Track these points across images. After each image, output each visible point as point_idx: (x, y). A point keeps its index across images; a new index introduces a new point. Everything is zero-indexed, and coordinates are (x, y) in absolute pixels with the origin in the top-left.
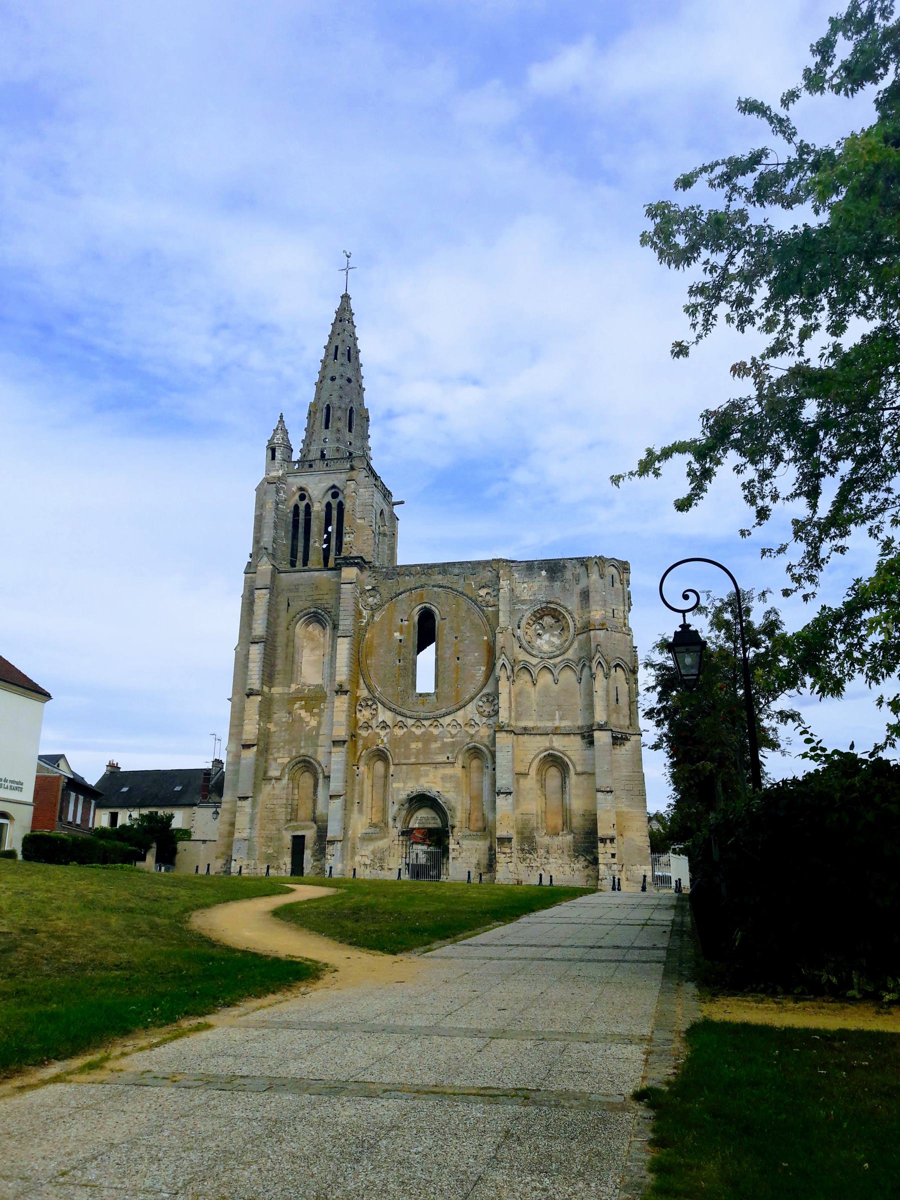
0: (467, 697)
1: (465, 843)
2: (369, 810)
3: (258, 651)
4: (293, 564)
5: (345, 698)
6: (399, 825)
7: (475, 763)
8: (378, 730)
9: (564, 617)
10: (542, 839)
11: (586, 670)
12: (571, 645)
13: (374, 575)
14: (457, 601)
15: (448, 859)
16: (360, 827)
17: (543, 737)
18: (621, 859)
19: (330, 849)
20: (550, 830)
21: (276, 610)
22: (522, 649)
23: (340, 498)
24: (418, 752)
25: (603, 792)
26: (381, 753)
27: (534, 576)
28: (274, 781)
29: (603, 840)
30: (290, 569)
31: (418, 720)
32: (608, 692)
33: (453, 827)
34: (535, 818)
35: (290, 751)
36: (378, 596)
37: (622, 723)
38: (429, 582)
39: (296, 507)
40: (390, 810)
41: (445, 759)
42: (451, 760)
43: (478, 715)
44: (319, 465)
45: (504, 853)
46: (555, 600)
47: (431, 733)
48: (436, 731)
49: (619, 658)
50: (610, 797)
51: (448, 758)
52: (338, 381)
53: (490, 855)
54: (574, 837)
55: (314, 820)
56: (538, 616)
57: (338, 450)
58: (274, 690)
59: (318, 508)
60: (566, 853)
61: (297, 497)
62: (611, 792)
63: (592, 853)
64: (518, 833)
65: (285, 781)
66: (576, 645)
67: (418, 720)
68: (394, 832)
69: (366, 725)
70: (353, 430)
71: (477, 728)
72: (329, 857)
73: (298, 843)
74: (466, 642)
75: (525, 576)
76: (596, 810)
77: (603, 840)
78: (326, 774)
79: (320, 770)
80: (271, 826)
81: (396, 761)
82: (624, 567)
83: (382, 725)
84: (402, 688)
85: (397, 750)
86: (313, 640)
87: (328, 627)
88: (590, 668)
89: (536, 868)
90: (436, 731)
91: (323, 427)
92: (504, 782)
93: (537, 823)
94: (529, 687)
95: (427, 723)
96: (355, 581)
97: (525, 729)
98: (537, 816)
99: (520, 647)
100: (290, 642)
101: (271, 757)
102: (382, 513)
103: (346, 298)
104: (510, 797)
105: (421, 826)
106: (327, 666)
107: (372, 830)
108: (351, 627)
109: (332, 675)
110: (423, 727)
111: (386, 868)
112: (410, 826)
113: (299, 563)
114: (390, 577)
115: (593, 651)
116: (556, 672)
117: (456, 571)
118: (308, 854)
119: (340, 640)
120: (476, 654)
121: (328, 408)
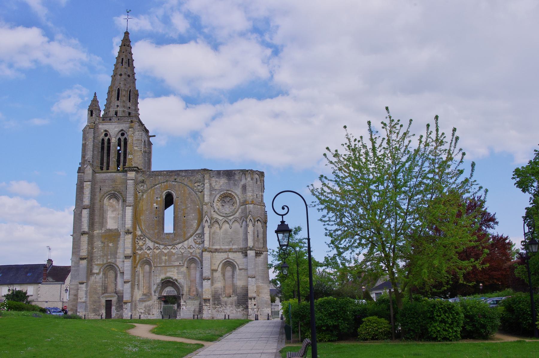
1: (189, 302)
2: (142, 287)
3: (87, 213)
4: (102, 168)
5: (130, 236)
6: (157, 294)
7: (193, 265)
8: (146, 251)
9: (235, 197)
10: (224, 299)
11: (244, 222)
12: (238, 211)
13: (143, 175)
15: (180, 309)
17: (224, 253)
18: (258, 307)
19: (125, 306)
20: (226, 294)
21: (94, 191)
23: (125, 136)
24: (166, 261)
25: (251, 277)
26: (148, 261)
28: (95, 275)
29: (251, 299)
30: (100, 171)
32: (254, 233)
33: (182, 295)
35: (103, 261)
37: (260, 246)
39: (103, 140)
40: (153, 288)
41: (179, 264)
44: (115, 119)
45: (206, 306)
46: (231, 189)
47: (172, 252)
48: (174, 251)
49: (259, 217)
50: (254, 279)
52: (123, 76)
53: (200, 307)
54: (238, 297)
55: (116, 293)
56: (223, 196)
57: (124, 111)
58: (95, 232)
59: (114, 140)
60: (234, 305)
61: (103, 135)
62: (255, 277)
63: (246, 304)
64: (212, 297)
65: (101, 275)
66: (240, 211)
68: (155, 297)
69: (140, 248)
70: (131, 101)
71: (194, 250)
72: (125, 310)
73: (109, 304)
74: (188, 209)
75: (217, 178)
76: (248, 285)
77: (251, 299)
78: (121, 271)
79: (118, 270)
80: (95, 296)
82: (262, 174)
86: (112, 207)
87: (120, 201)
88: (246, 222)
89: (220, 312)
91: (116, 99)
93: (221, 292)
95: (170, 247)
96: (134, 179)
97: (216, 249)
98: (221, 289)
99: (214, 212)
100: (102, 207)
101: (94, 263)
102: (145, 141)
104: (210, 281)
105: (167, 294)
106: (120, 220)
107: (144, 297)
109: (124, 224)
111: (151, 314)
112: (162, 295)
113: (105, 168)
115: (248, 214)
116: (231, 224)
118: (113, 308)
119: (127, 208)
120: (193, 215)
121: (119, 90)
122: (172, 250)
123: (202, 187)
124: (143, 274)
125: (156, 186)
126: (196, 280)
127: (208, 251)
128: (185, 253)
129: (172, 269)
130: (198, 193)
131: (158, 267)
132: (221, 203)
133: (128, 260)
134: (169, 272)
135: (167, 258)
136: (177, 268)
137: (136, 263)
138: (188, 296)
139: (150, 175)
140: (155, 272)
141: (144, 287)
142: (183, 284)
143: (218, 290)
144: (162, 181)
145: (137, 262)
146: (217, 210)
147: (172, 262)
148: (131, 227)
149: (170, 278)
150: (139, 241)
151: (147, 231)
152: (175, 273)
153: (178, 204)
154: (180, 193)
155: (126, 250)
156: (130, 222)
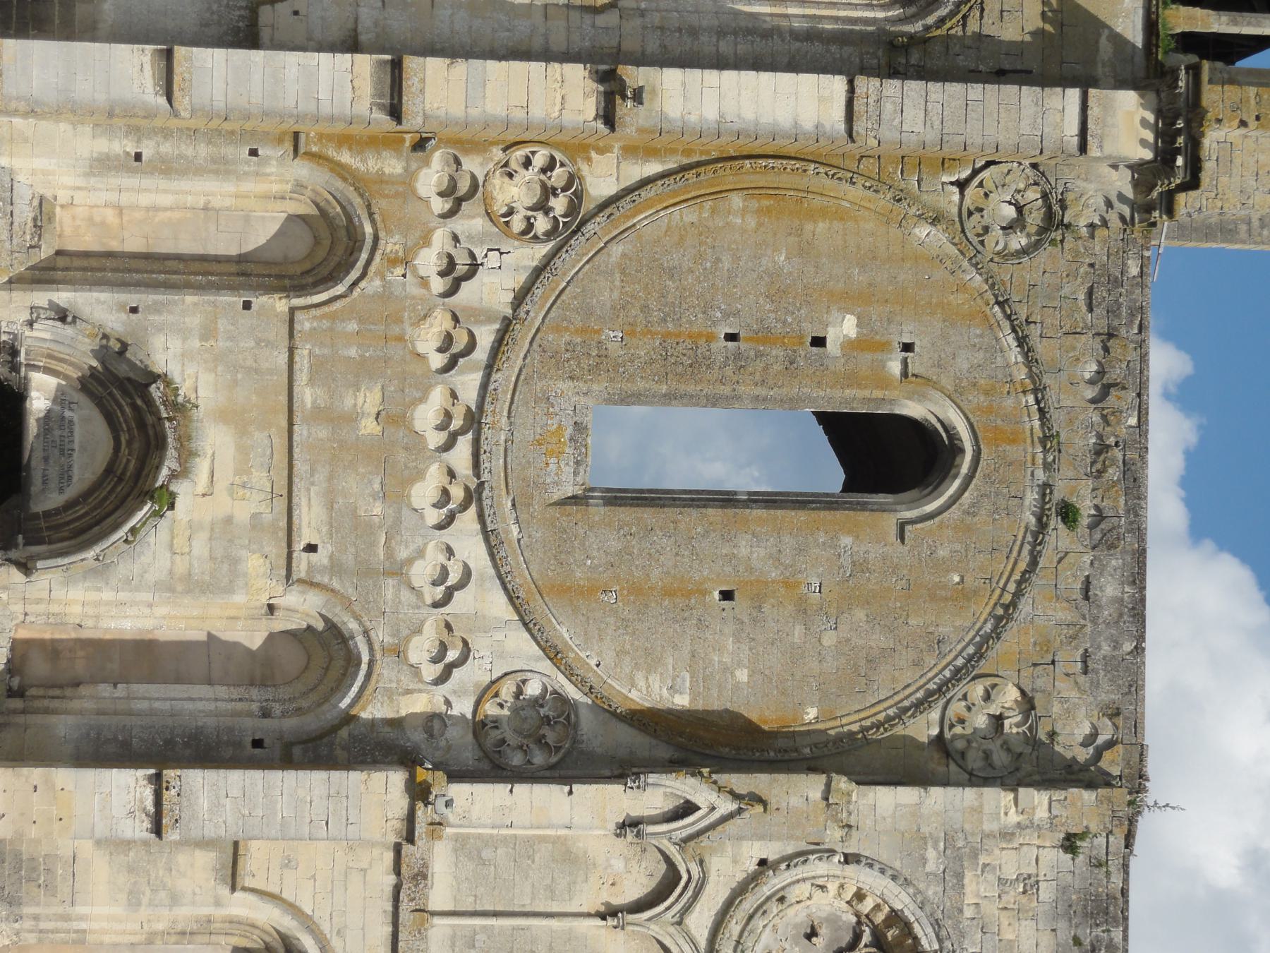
0: (564, 632)
2: (113, 197)
8: (440, 239)
14: (976, 592)
16: (39, 163)
22: (752, 867)
27: (1062, 925)
31: (474, 420)
33: (26, 567)
34: (60, 910)
36: (1019, 241)
38: (1065, 471)
42: (302, 562)
43: (487, 679)
47: (420, 475)
51: (311, 548)
56: (891, 934)
67: (474, 420)
74: (798, 630)
75: (1063, 890)
81: (305, 323)
83: (462, 261)
84: (614, 348)
85: (353, 326)
90: (424, 493)
92: (204, 803)
93: (36, 918)
94: (592, 897)
95: (461, 455)
96: (1093, 151)
97: (422, 876)
98: (66, 918)
99: (763, 862)
104: (139, 828)
107: (24, 212)
108: (888, 134)
110: (441, 438)
112: (37, 378)
114: (1100, 293)
117: (1109, 589)
120: (742, 675)
123: (987, 755)
124: (228, 202)
125: (1011, 340)
126: (151, 681)
127: (411, 818)
128: (406, 595)
129: (260, 478)
130: (935, 715)
131: (291, 351)
132: (833, 920)
133: (366, 88)
134: (243, 451)
135: (369, 426)
136: (268, 517)
137: (331, 152)
138: (18, 608)
139: (1118, 283)
140: (246, 318)
141: (120, 210)
142: (123, 569)
143: (50, 889)
144: (1052, 396)
145: (346, 157)
146: (774, 882)
147: (330, 478)
148: (663, 116)
149: (187, 455)
150: (531, 174)
151: (617, 250)
152: (222, 504)
153: (846, 541)
154: (942, 553)
155: (462, 67)
156: (711, 114)
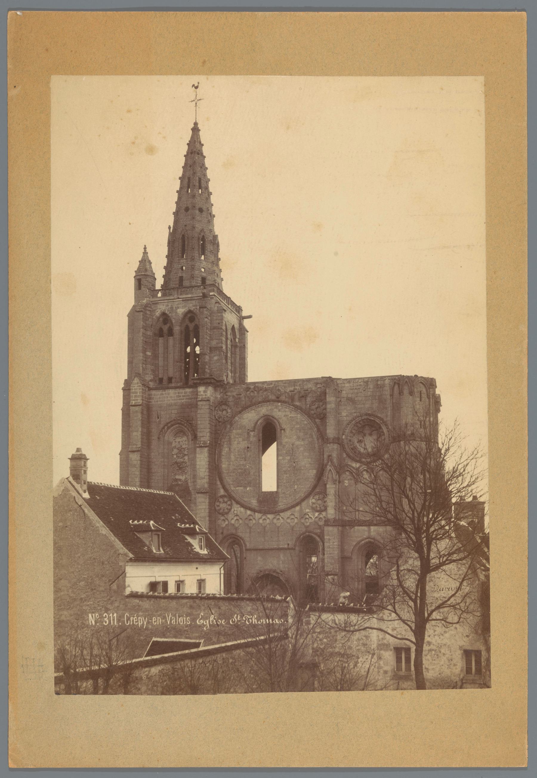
103: (195, 130)
122: (275, 521)
